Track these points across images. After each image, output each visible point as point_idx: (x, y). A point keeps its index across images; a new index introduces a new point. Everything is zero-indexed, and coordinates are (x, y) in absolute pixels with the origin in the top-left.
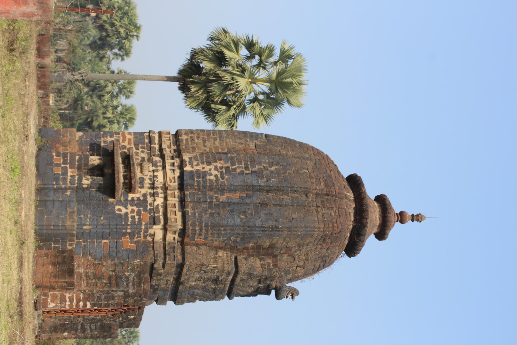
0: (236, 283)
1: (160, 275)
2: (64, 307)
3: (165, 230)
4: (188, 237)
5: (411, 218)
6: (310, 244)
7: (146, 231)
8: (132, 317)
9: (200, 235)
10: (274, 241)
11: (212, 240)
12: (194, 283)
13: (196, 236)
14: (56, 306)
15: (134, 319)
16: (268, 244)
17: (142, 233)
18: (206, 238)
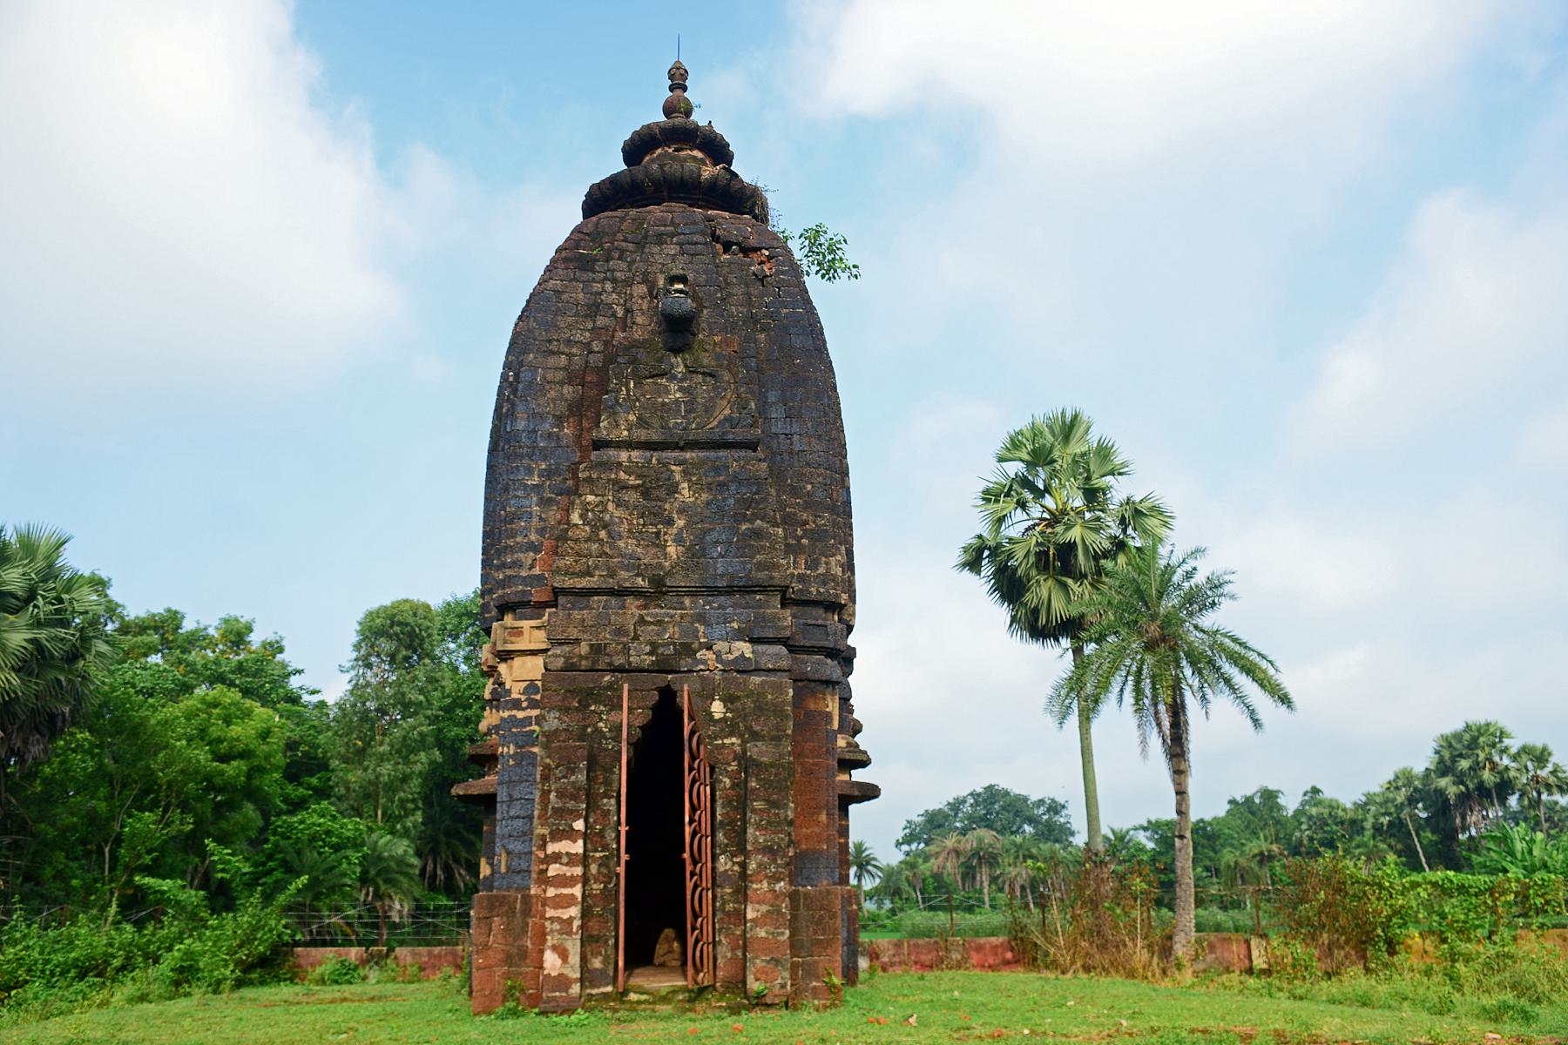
0: (655, 437)
1: (597, 649)
2: (571, 919)
3: (505, 656)
4: (524, 592)
5: (678, 92)
6: (597, 287)
7: (516, 705)
8: (717, 708)
9: (517, 564)
10: (560, 375)
11: (541, 532)
12: (671, 550)
13: (524, 574)
14: (554, 948)
15: (728, 700)
16: (567, 390)
17: (520, 715)
18: (535, 548)
